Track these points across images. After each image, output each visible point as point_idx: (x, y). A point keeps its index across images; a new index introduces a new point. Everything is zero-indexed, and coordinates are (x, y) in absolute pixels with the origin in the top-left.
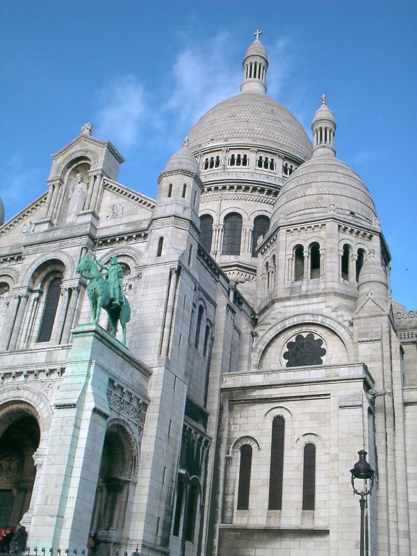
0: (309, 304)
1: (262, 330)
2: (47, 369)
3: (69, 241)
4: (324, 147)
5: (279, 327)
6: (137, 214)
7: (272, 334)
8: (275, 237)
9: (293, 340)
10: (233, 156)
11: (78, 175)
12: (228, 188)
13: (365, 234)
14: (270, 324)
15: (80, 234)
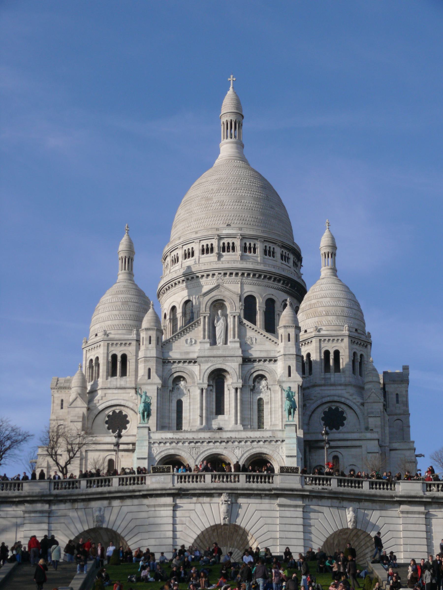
0: (336, 390)
1: (309, 403)
2: (275, 440)
3: (230, 358)
4: (331, 269)
5: (319, 402)
6: (264, 345)
7: (315, 405)
8: (310, 341)
9: (327, 410)
10: (245, 244)
11: (219, 312)
12: (246, 275)
13: (364, 344)
14: (313, 400)
15: (236, 355)
